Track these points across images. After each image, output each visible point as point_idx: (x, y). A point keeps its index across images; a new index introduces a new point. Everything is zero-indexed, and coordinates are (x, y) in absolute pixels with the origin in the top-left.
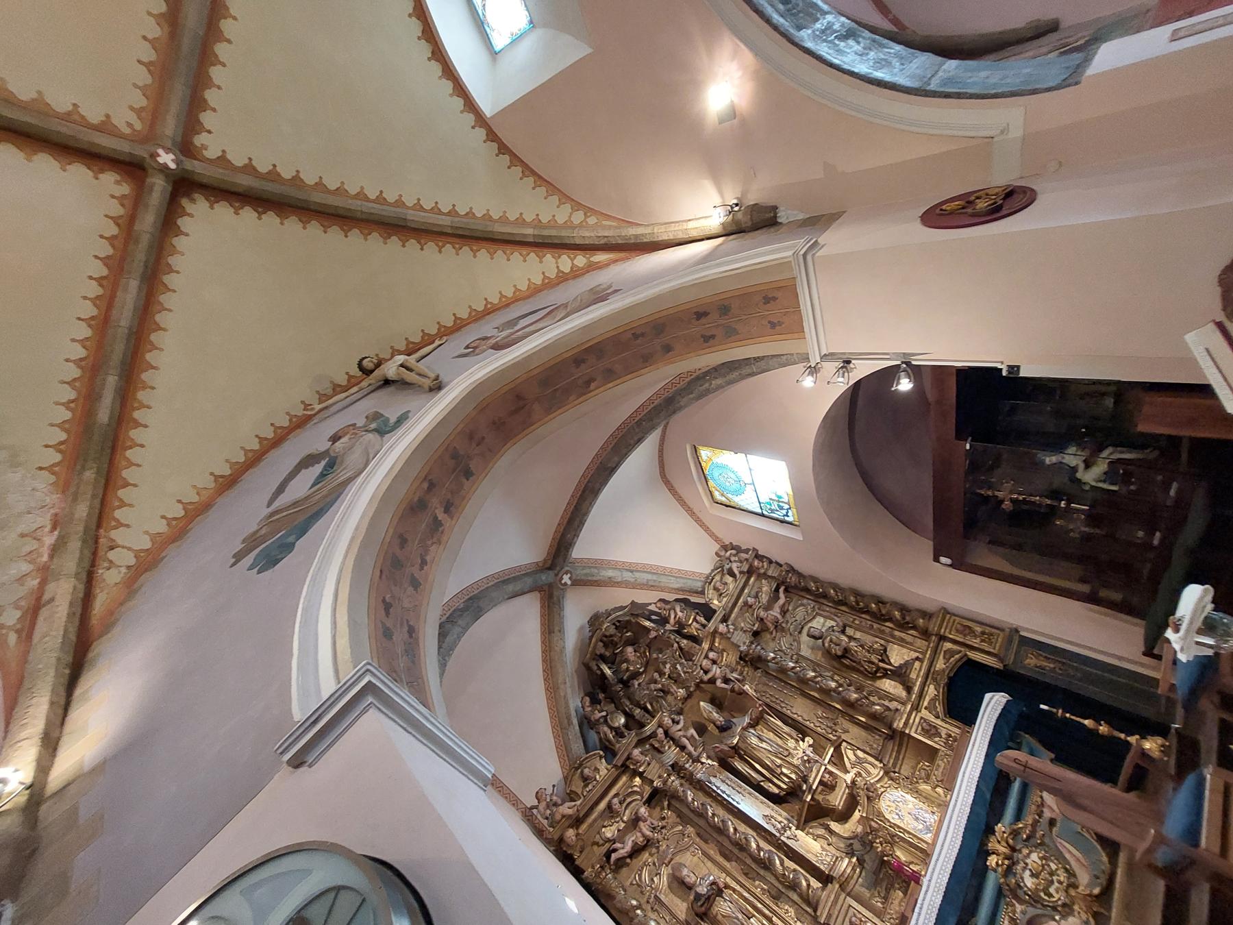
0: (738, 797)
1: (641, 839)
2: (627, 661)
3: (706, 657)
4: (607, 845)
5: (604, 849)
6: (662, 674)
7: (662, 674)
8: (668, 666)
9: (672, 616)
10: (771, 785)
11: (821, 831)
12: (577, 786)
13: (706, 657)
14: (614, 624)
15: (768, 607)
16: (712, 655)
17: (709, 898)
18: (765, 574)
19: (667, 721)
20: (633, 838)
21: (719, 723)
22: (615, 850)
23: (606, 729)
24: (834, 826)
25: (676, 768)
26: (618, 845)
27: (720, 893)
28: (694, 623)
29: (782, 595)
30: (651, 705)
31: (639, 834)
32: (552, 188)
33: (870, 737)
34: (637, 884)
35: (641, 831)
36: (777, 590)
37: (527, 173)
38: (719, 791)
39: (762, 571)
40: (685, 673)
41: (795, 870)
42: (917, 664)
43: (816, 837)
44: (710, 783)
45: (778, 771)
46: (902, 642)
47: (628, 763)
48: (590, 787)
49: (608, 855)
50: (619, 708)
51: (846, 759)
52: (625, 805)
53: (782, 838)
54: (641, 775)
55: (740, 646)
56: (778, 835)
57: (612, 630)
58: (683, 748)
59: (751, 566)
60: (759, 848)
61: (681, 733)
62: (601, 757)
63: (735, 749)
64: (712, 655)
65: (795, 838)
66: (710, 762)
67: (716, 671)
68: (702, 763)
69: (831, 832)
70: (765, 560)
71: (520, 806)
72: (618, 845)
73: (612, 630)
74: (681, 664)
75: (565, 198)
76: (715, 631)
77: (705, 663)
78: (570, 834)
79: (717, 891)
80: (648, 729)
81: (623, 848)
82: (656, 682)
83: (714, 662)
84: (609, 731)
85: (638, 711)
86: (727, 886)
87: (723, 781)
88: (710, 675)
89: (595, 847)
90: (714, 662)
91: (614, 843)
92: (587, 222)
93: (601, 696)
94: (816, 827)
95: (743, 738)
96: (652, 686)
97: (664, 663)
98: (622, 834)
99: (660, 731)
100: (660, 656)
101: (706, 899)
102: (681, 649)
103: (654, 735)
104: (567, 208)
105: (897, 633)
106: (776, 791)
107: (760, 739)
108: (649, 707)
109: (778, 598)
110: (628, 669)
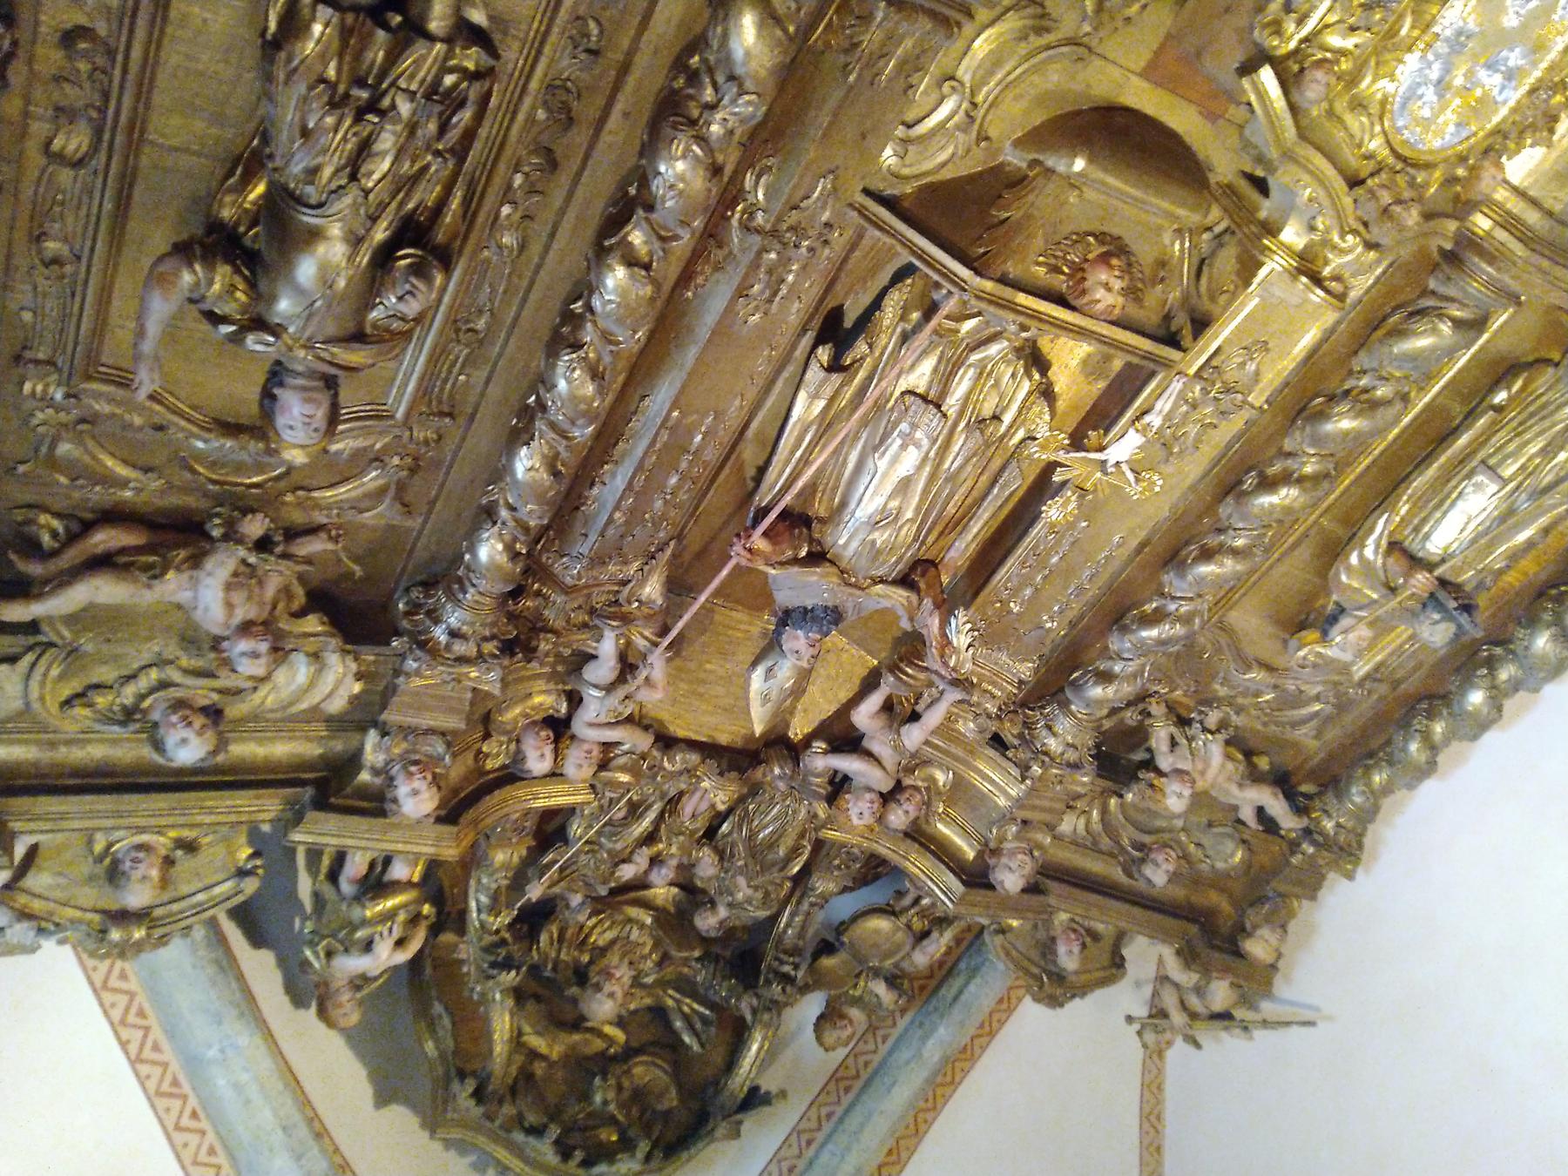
1: (1230, 766)
13: (555, 775)
20: (1234, 789)
26: (1247, 815)
35: (1215, 778)
52: (1147, 839)
72: (1247, 815)
77: (578, 765)
99: (898, 818)
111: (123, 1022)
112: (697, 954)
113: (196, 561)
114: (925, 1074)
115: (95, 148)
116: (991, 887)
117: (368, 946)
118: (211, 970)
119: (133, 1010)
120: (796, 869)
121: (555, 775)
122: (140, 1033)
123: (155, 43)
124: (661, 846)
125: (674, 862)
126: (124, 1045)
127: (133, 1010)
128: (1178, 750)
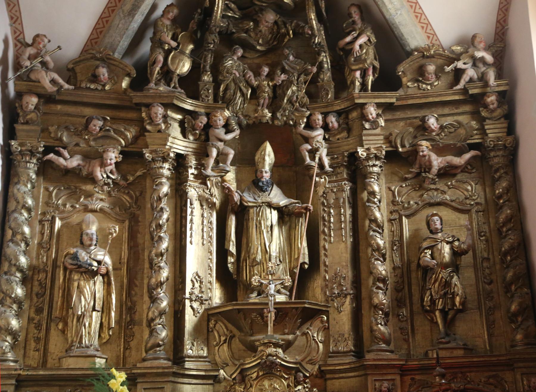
2: (257, 23)
3: (325, 115)
4: (57, 143)
6: (270, 76)
7: (270, 76)
9: (348, 39)
17: (80, 266)
18: (484, 119)
22: (59, 154)
23: (161, 58)
26: (66, 153)
36: (472, 147)
38: (189, 218)
39: (484, 114)
44: (191, 204)
47: (143, 109)
53: (187, 302)
55: (362, 146)
56: (187, 295)
59: (483, 95)
70: (506, 107)
71: (17, 25)
81: (65, 159)
82: (257, 74)
84: (160, 65)
85: (207, 78)
87: (202, 216)
90: (326, 127)
91: (64, 148)
100: (291, 58)
101: (77, 264)
109: (459, 153)
110: (247, 31)
111: (421, 14)
112: (236, 35)
113: (439, 170)
114: (140, 10)
115: (482, 263)
116: (162, 104)
117: (361, 46)
118: (403, 38)
119: (419, 18)
120: (222, 86)
122: (416, 11)
125: (263, 77)
126: (420, 8)
127: (419, 18)
128: (109, 171)
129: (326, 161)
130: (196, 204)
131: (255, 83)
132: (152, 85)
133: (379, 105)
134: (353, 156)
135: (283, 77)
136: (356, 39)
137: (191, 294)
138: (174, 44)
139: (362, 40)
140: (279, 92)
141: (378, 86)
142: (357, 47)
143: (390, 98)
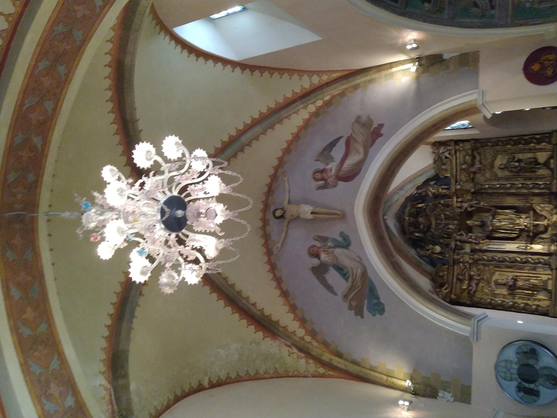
0: (503, 247)
5: (466, 292)
6: (441, 220)
8: (442, 215)
9: (430, 193)
10: (512, 235)
11: (540, 240)
12: (440, 281)
14: (410, 216)
15: (473, 164)
16: (459, 200)
19: (458, 237)
21: (479, 225)
22: (471, 290)
23: (436, 255)
24: (544, 236)
25: (473, 251)
26: (471, 288)
27: (516, 280)
28: (443, 191)
29: (477, 155)
30: (446, 234)
31: (475, 281)
32: (291, 72)
33: (543, 198)
34: (485, 294)
37: (272, 72)
40: (451, 213)
41: (538, 259)
42: (552, 161)
43: (538, 244)
45: (513, 229)
46: (541, 150)
48: (445, 278)
49: (469, 293)
50: (435, 244)
51: (537, 211)
54: (461, 262)
57: (412, 220)
58: (470, 242)
60: (521, 259)
61: (467, 238)
62: (441, 266)
63: (492, 231)
64: (459, 200)
65: (532, 248)
66: (485, 241)
67: (465, 205)
68: (482, 243)
69: (543, 238)
73: (412, 220)
74: (447, 211)
75: (301, 72)
76: (456, 190)
77: (459, 205)
78: (453, 296)
79: (515, 280)
80: (453, 245)
81: (473, 288)
82: (440, 224)
83: (461, 202)
86: (517, 276)
88: (464, 209)
89: (463, 294)
92: (322, 80)
93: (422, 244)
94: (537, 240)
95: (492, 225)
96: (441, 227)
97: (440, 215)
98: (469, 285)
99: (458, 243)
102: (442, 205)
103: (456, 245)
104: (306, 77)
105: (537, 147)
106: (515, 235)
107: (500, 222)
108: (446, 236)
110: (424, 227)
121: (457, 202)
123: (527, 153)
124: (444, 220)
129: (474, 202)
130: (490, 246)
131: (444, 225)
132: (445, 258)
133: (456, 185)
134: (473, 193)
135: (442, 215)
136: (430, 191)
137: (525, 249)
138: (430, 251)
139: (431, 189)
140: (447, 217)
141: (448, 184)
142: (433, 191)
143: (453, 181)
